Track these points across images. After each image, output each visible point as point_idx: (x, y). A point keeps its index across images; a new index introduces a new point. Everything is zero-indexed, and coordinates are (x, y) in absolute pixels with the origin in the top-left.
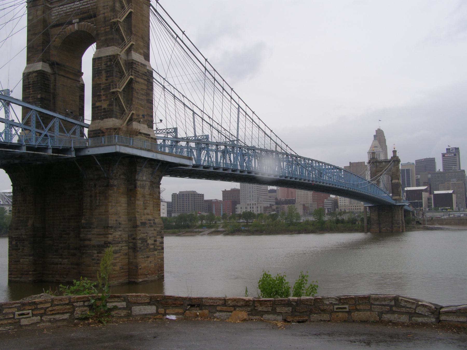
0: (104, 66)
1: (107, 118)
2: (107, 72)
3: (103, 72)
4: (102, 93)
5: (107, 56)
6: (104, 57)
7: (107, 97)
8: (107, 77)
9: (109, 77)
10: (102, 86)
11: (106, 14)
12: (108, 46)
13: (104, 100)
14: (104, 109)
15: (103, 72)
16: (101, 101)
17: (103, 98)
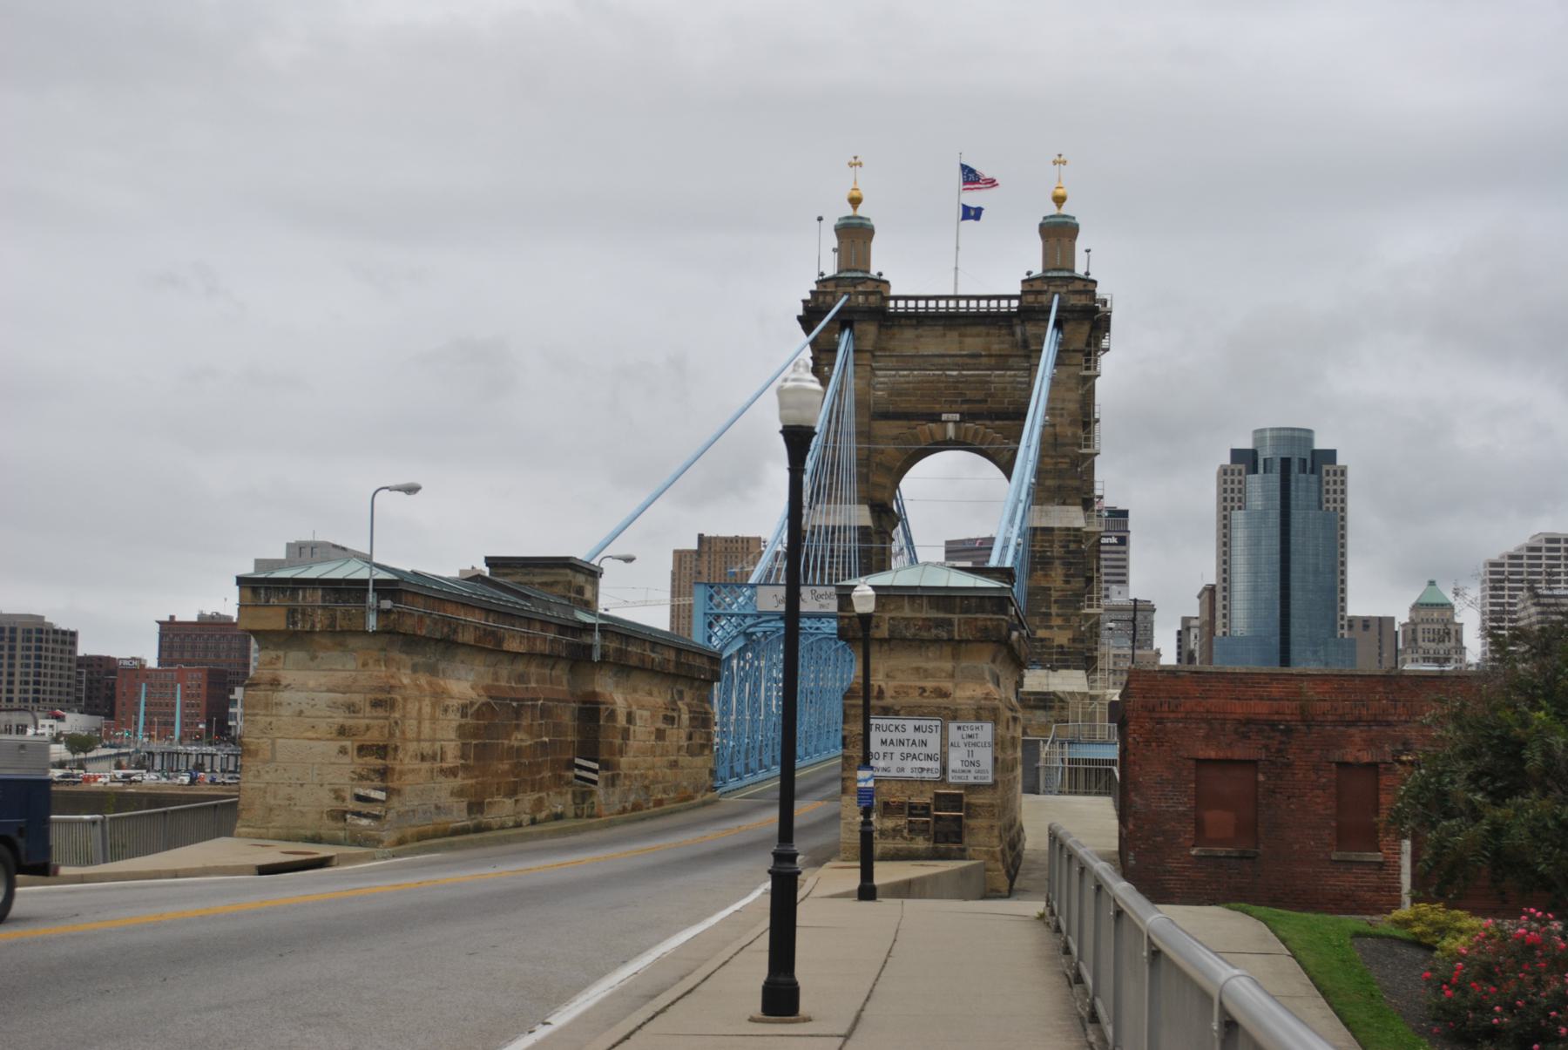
0: (1057, 550)
1: (1067, 667)
2: (1067, 564)
3: (1057, 562)
4: (1054, 610)
5: (1068, 529)
6: (1060, 529)
7: (1067, 620)
8: (1066, 575)
9: (1073, 576)
10: (1055, 595)
11: (1058, 429)
12: (1064, 504)
13: (1060, 627)
14: (1061, 646)
15: (1057, 562)
16: (1051, 627)
17: (1057, 622)
